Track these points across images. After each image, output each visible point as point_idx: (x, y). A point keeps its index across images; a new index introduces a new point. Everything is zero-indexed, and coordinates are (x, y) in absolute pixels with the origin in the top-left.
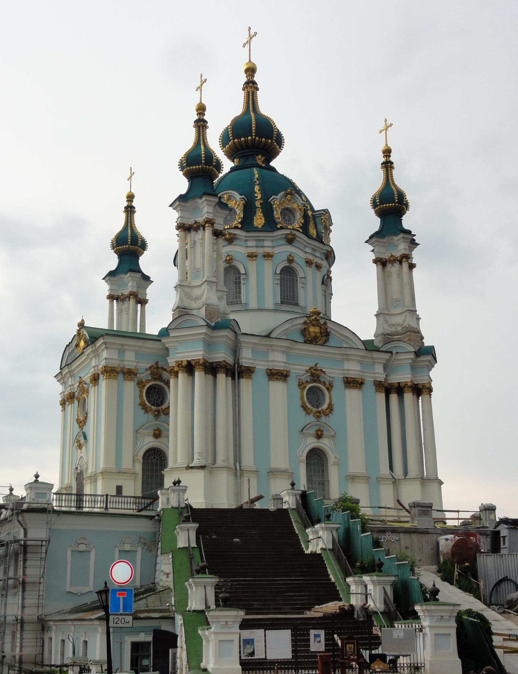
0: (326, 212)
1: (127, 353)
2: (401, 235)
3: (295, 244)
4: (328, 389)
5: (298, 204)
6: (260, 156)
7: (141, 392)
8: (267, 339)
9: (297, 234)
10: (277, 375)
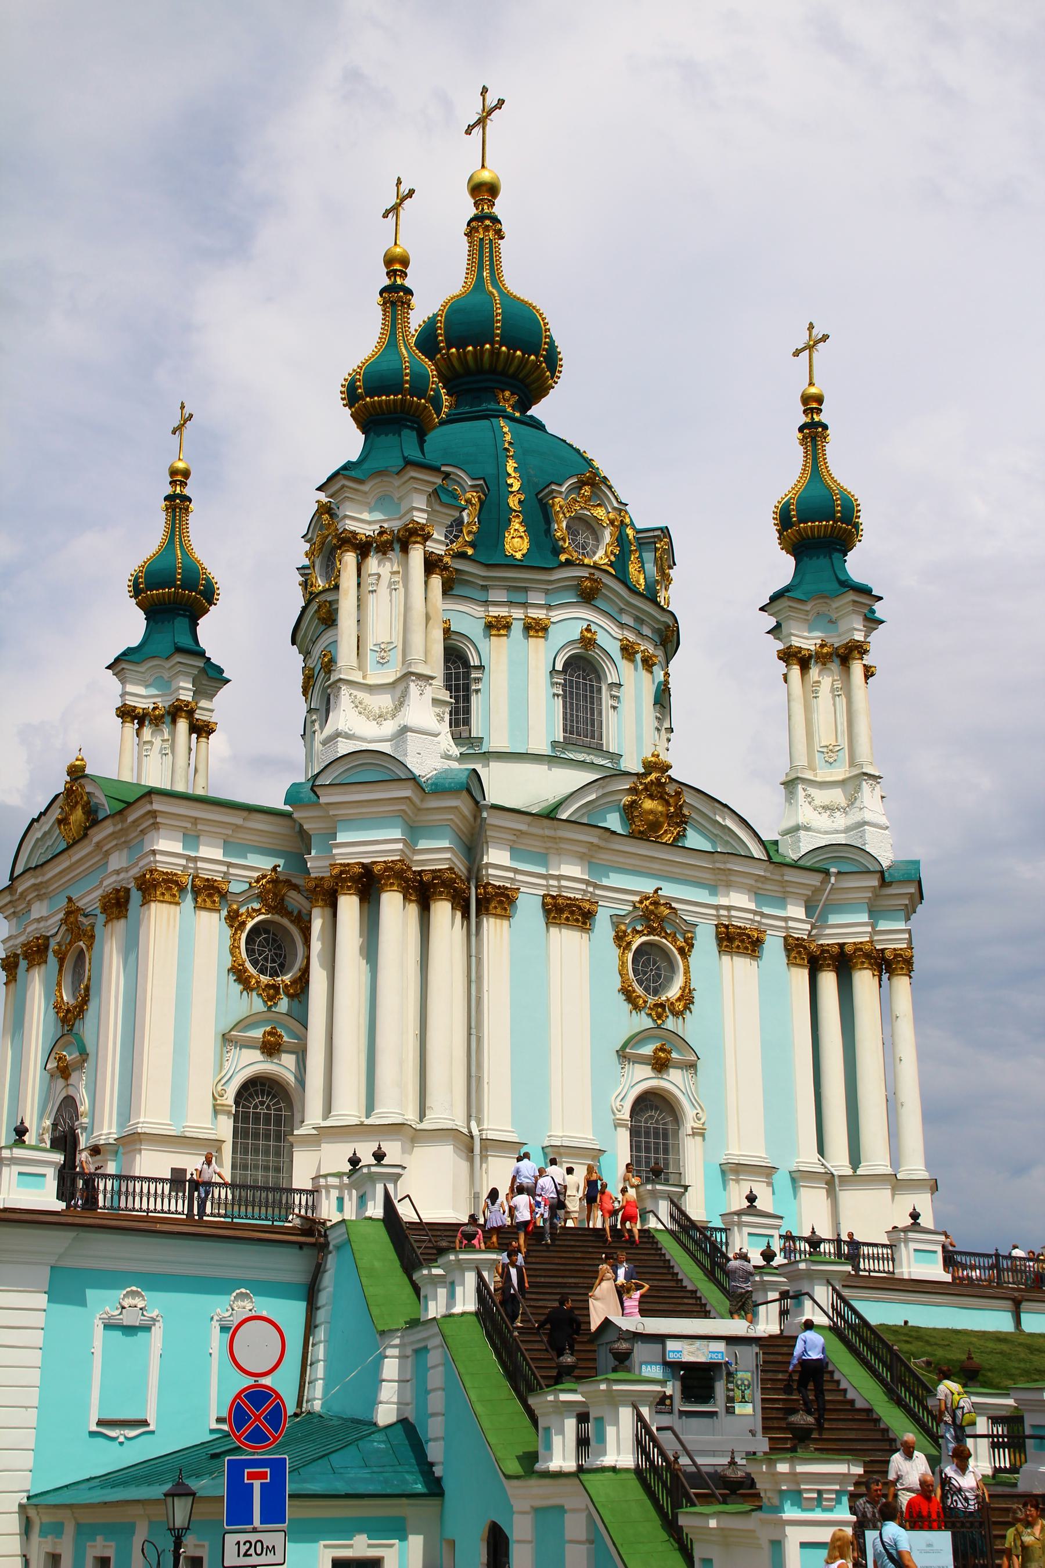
2: (851, 596)
3: (598, 603)
4: (681, 950)
5: (606, 509)
6: (507, 394)
7: (234, 938)
8: (546, 822)
9: (607, 580)
10: (567, 912)
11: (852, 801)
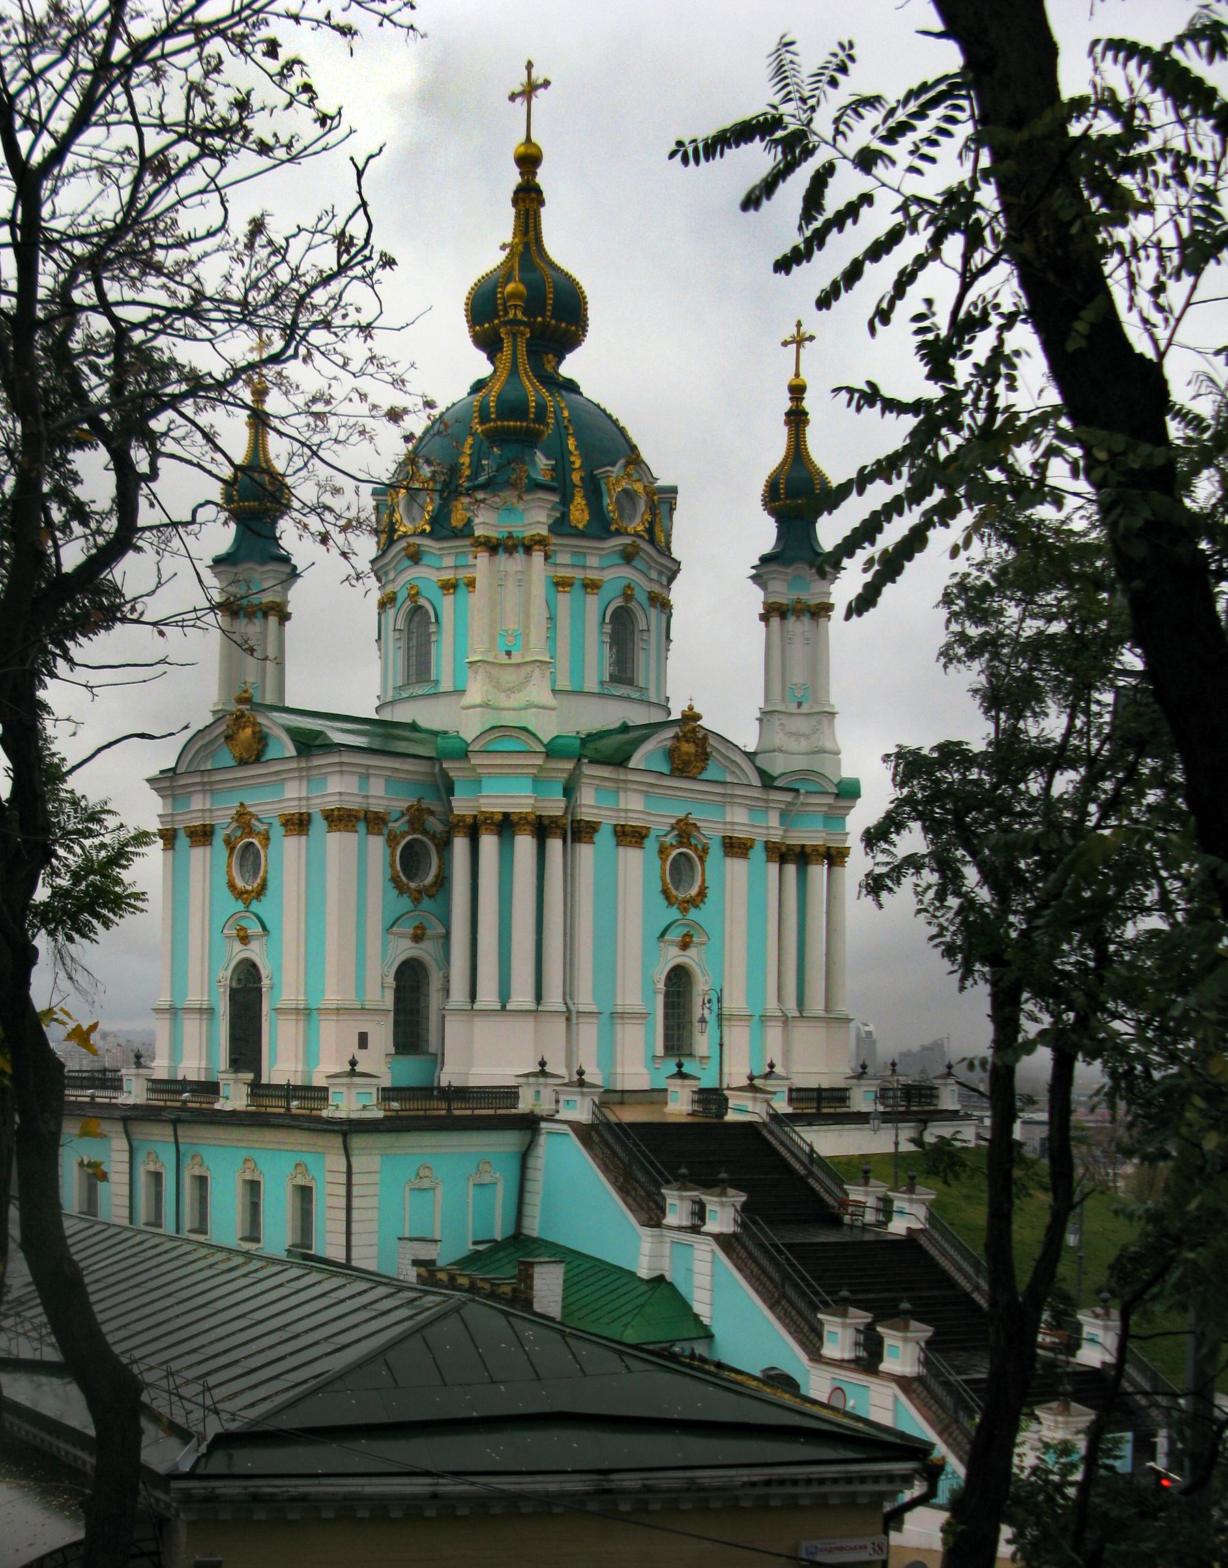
0: (674, 490)
1: (372, 780)
3: (634, 563)
4: (702, 860)
7: (393, 855)
8: (621, 770)
10: (629, 836)
11: (815, 731)
